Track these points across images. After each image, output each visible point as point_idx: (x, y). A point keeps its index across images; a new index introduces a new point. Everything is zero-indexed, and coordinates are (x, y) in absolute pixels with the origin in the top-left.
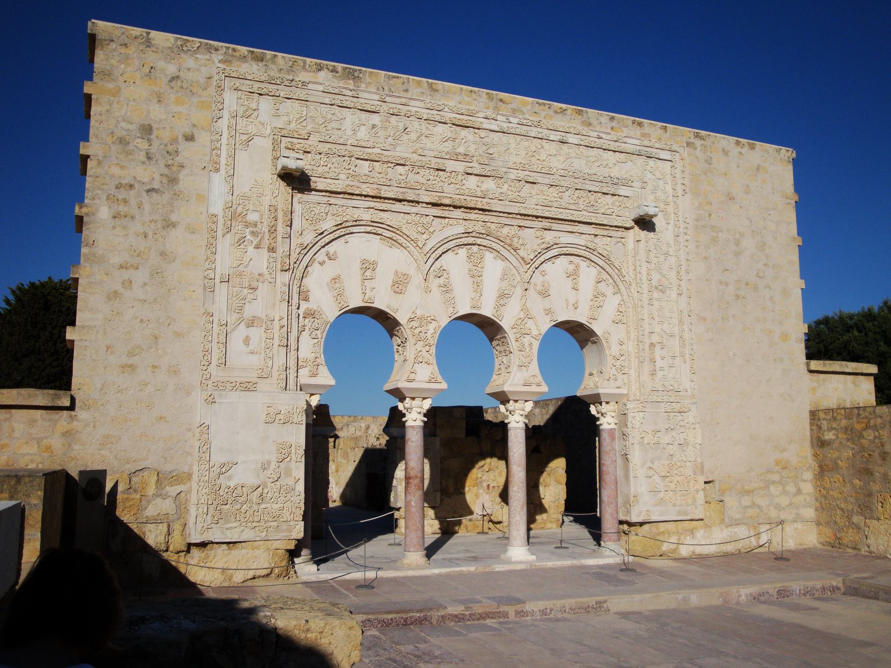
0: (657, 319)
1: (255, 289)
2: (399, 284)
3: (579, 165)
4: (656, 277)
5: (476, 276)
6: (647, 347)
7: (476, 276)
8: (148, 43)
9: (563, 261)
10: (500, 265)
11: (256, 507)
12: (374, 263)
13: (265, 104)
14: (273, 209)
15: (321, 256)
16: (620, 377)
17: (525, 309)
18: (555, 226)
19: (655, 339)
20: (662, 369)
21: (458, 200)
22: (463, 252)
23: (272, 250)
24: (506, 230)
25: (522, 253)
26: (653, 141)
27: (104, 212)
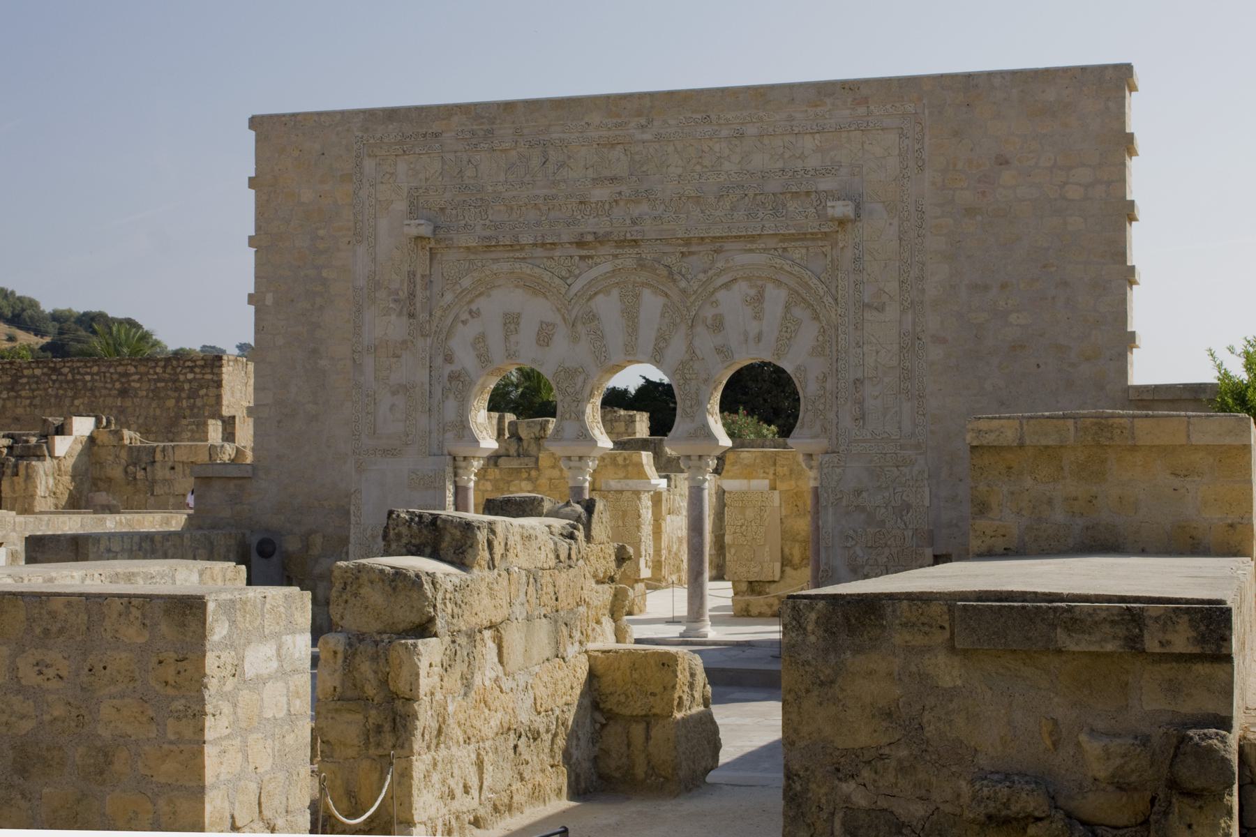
1: (398, 357)
5: (631, 315)
7: (631, 315)
10: (660, 301)
12: (519, 315)
14: (412, 274)
17: (691, 350)
18: (728, 246)
23: (411, 316)
25: (683, 284)
26: (872, 107)
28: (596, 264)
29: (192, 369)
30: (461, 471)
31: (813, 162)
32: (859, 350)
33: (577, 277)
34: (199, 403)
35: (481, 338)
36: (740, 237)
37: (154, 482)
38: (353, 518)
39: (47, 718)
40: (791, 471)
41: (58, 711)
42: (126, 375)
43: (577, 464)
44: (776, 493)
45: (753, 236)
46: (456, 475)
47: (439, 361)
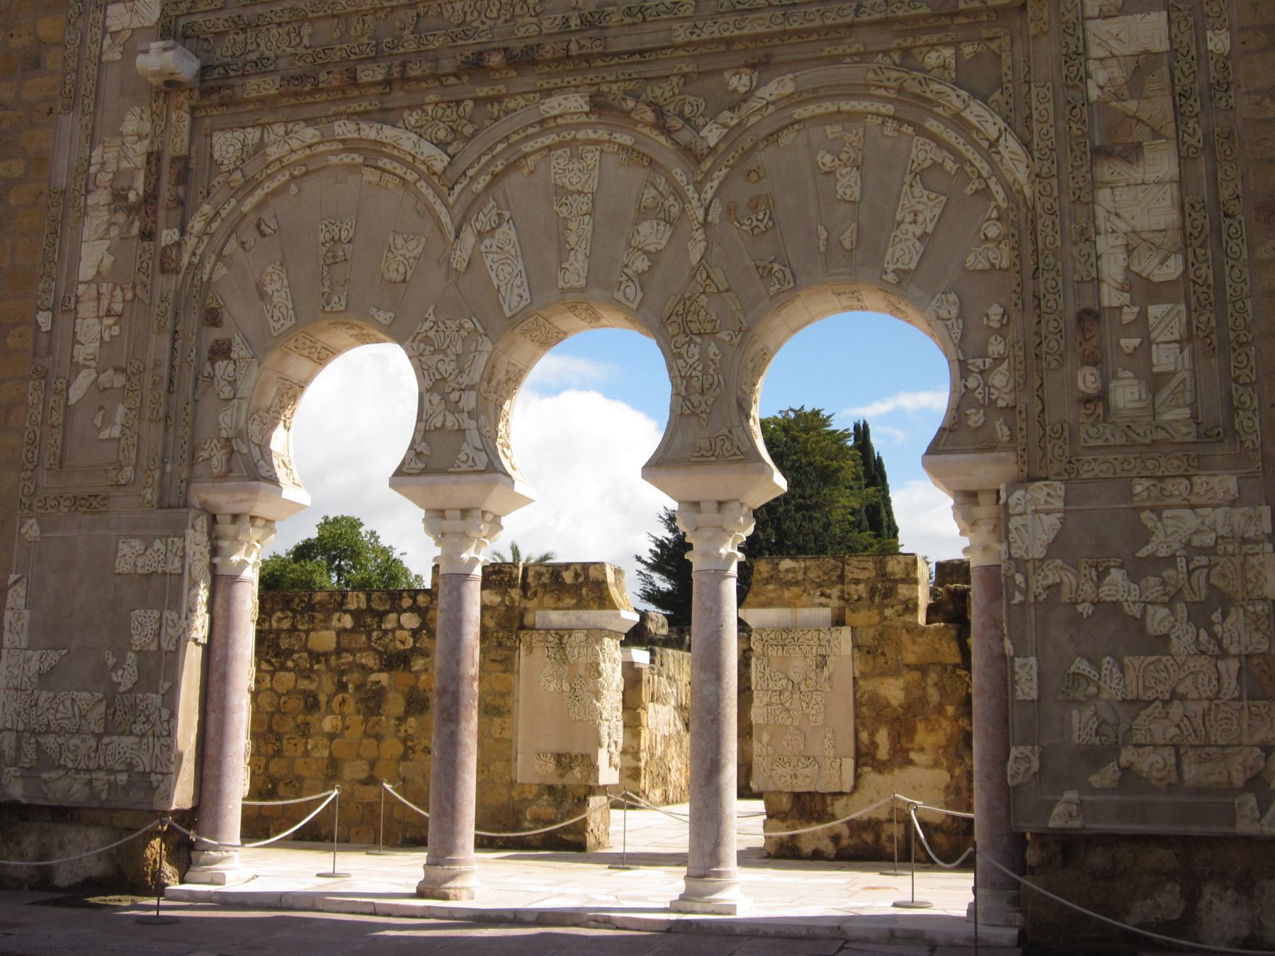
11: (93, 743)
25: (686, 136)
28: (506, 113)
30: (225, 544)
32: (1086, 248)
33: (468, 139)
36: (809, 32)
38: (6, 635)
40: (873, 591)
43: (458, 525)
44: (846, 632)
45: (836, 28)
46: (214, 551)
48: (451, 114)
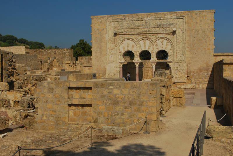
0: (178, 48)
2: (133, 47)
3: (163, 23)
4: (178, 40)
5: (145, 44)
6: (176, 53)
7: (145, 44)
8: (98, 18)
9: (160, 39)
13: (113, 23)
15: (121, 44)
16: (171, 58)
19: (177, 52)
20: (179, 57)
21: (141, 33)
22: (143, 41)
23: (114, 44)
24: (150, 36)
27: (94, 42)
29: (65, 50)
31: (170, 23)
34: (66, 55)
35: (124, 47)
37: (62, 66)
39: (134, 98)
41: (136, 97)
42: (55, 51)
47: (118, 50)
48: (136, 37)
